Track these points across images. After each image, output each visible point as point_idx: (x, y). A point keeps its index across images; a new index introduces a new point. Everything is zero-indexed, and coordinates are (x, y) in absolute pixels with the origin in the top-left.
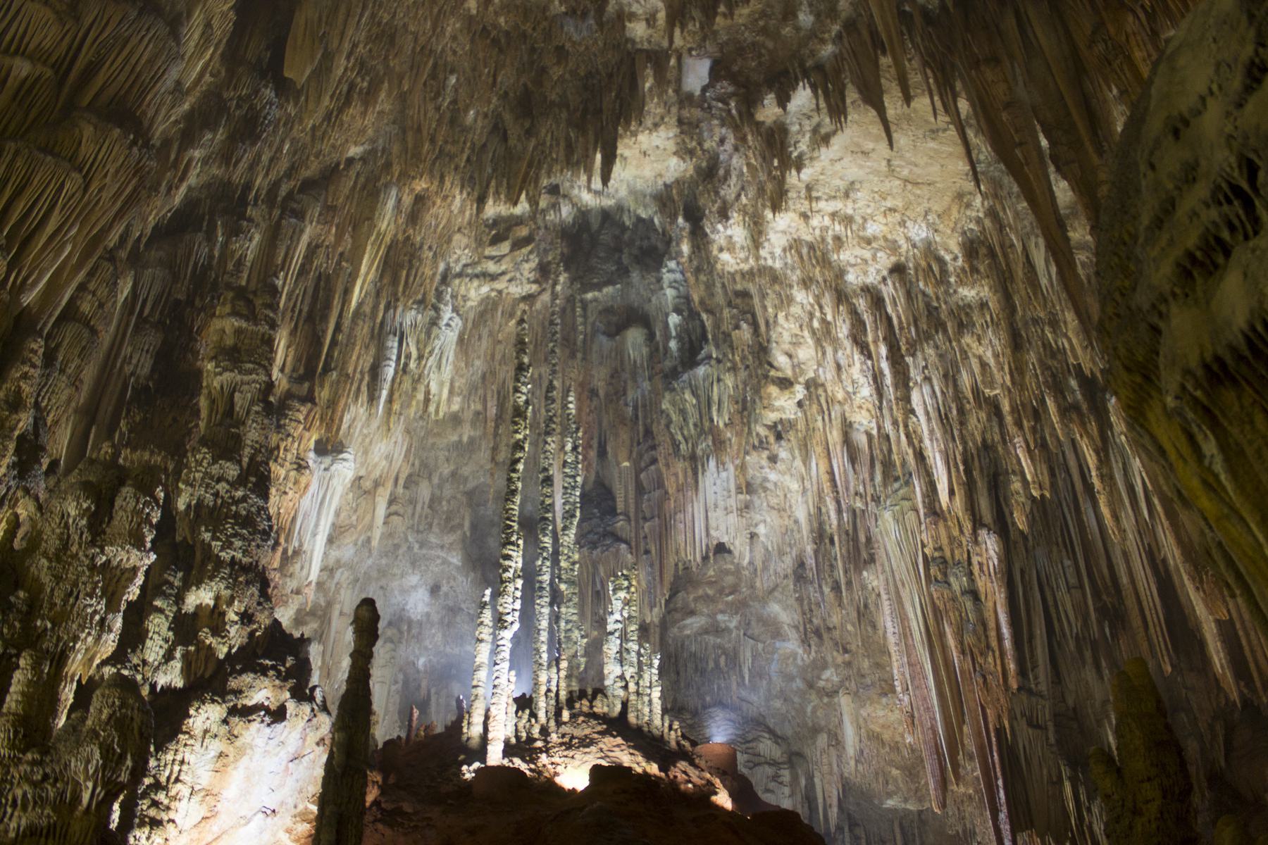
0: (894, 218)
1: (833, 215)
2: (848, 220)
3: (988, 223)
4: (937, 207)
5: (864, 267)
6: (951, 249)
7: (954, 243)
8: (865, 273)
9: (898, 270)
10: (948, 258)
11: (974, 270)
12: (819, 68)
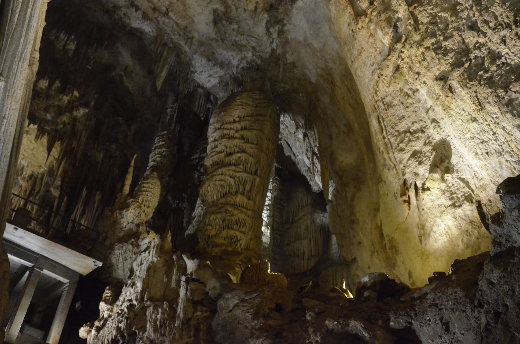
3: (40, 176)
4: (33, 163)
6: (27, 172)
10: (24, 173)
11: (28, 181)
12: (43, 129)
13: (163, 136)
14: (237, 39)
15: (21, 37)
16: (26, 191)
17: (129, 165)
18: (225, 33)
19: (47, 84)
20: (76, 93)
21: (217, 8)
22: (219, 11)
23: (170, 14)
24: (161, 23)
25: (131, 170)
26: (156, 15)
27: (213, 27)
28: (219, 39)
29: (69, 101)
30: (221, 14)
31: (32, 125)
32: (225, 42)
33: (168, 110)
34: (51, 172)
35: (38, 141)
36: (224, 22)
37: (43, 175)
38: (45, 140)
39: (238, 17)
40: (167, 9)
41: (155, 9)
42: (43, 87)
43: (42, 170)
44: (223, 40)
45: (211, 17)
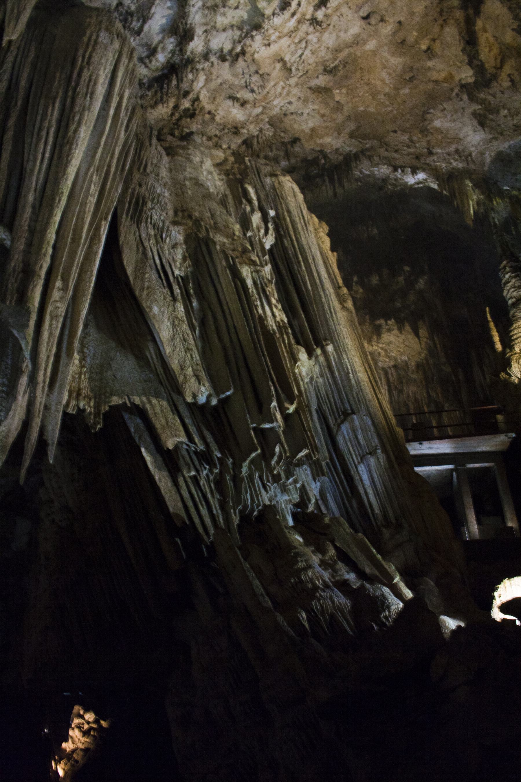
0: (399, 353)
1: (382, 348)
2: (386, 351)
3: (424, 361)
5: (385, 362)
6: (413, 364)
7: (413, 363)
8: (384, 364)
9: (395, 366)
11: (417, 372)
13: (504, 267)
14: (515, 122)
15: (321, 297)
16: (421, 382)
17: (488, 322)
18: (499, 125)
19: (377, 278)
20: (407, 268)
21: (475, 110)
22: (478, 112)
23: (434, 151)
24: (432, 164)
25: (492, 325)
26: (423, 161)
27: (482, 129)
28: (497, 136)
29: (405, 280)
30: (481, 112)
31: (389, 322)
32: (505, 133)
33: (494, 236)
34: (432, 352)
35: (403, 332)
36: (491, 116)
37: (426, 359)
38: (408, 328)
39: (500, 102)
40: (428, 149)
41: (418, 158)
42: (376, 282)
43: (423, 355)
44: (501, 134)
45: (475, 122)
